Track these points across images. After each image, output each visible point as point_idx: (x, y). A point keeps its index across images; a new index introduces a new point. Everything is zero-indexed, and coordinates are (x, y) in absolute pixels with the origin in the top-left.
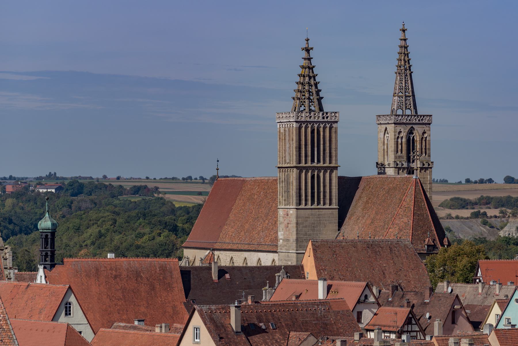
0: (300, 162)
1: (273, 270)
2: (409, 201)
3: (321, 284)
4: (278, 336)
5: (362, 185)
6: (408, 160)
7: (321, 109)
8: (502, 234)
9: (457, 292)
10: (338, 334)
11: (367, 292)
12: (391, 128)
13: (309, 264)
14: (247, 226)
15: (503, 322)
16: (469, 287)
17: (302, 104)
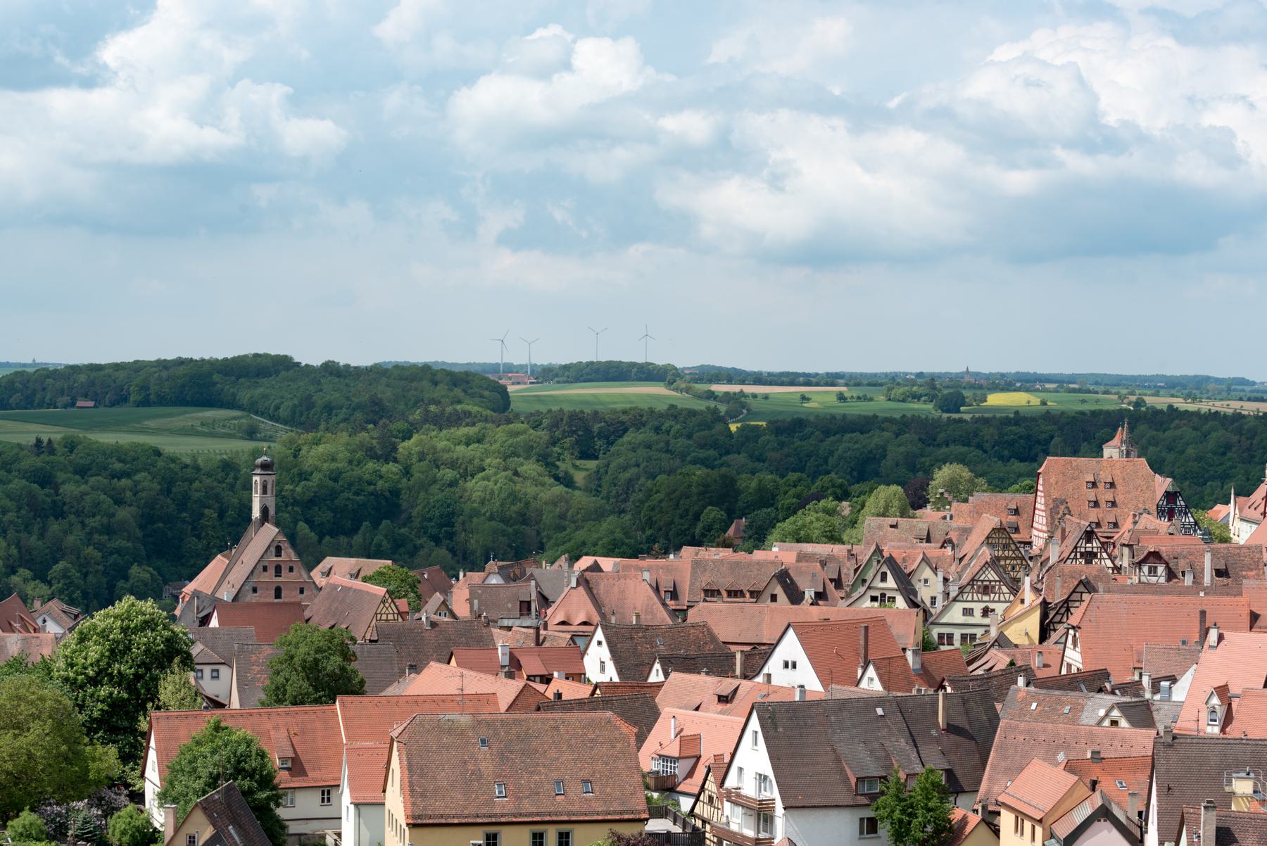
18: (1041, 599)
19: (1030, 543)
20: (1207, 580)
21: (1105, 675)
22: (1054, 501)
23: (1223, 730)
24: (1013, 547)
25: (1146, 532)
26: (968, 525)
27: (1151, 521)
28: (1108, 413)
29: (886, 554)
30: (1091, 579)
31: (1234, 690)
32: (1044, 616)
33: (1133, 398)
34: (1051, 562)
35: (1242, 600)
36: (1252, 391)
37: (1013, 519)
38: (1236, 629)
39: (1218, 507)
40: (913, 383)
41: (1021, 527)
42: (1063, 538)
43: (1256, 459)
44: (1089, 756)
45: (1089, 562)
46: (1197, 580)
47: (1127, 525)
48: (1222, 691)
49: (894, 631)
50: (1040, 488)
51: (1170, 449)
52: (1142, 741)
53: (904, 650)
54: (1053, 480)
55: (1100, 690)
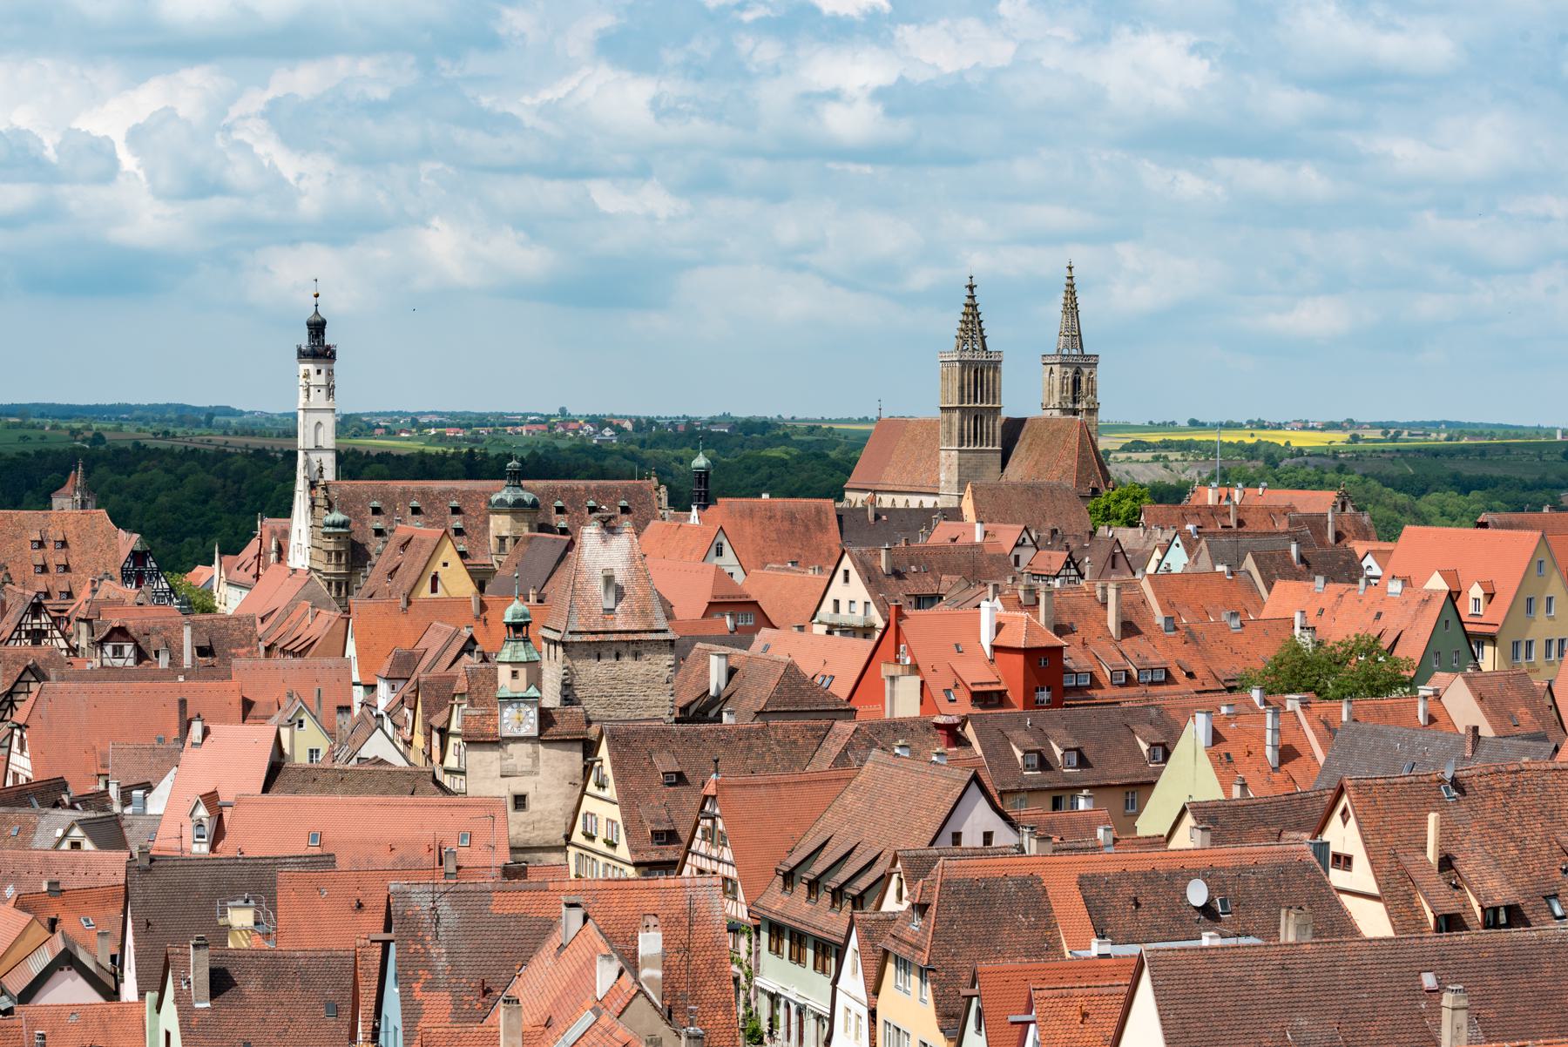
0: (962, 402)
1: (934, 510)
2: (1074, 441)
3: (978, 526)
4: (929, 579)
5: (1027, 426)
6: (1075, 401)
7: (984, 348)
8: (1183, 478)
9: (1118, 536)
10: (992, 578)
11: (1025, 535)
12: (1056, 368)
13: (968, 507)
14: (909, 468)
15: (1163, 565)
16: (1131, 531)
17: (965, 342)
20: (187, 660)
21: (61, 785)
23: (213, 849)
25: (109, 602)
27: (113, 589)
28: (58, 454)
31: (225, 796)
33: (89, 434)
35: (232, 685)
36: (242, 425)
38: (224, 720)
39: (199, 569)
43: (246, 508)
44: (45, 888)
45: (36, 642)
46: (175, 661)
47: (83, 595)
48: (211, 799)
51: (137, 497)
52: (111, 866)
55: (56, 805)
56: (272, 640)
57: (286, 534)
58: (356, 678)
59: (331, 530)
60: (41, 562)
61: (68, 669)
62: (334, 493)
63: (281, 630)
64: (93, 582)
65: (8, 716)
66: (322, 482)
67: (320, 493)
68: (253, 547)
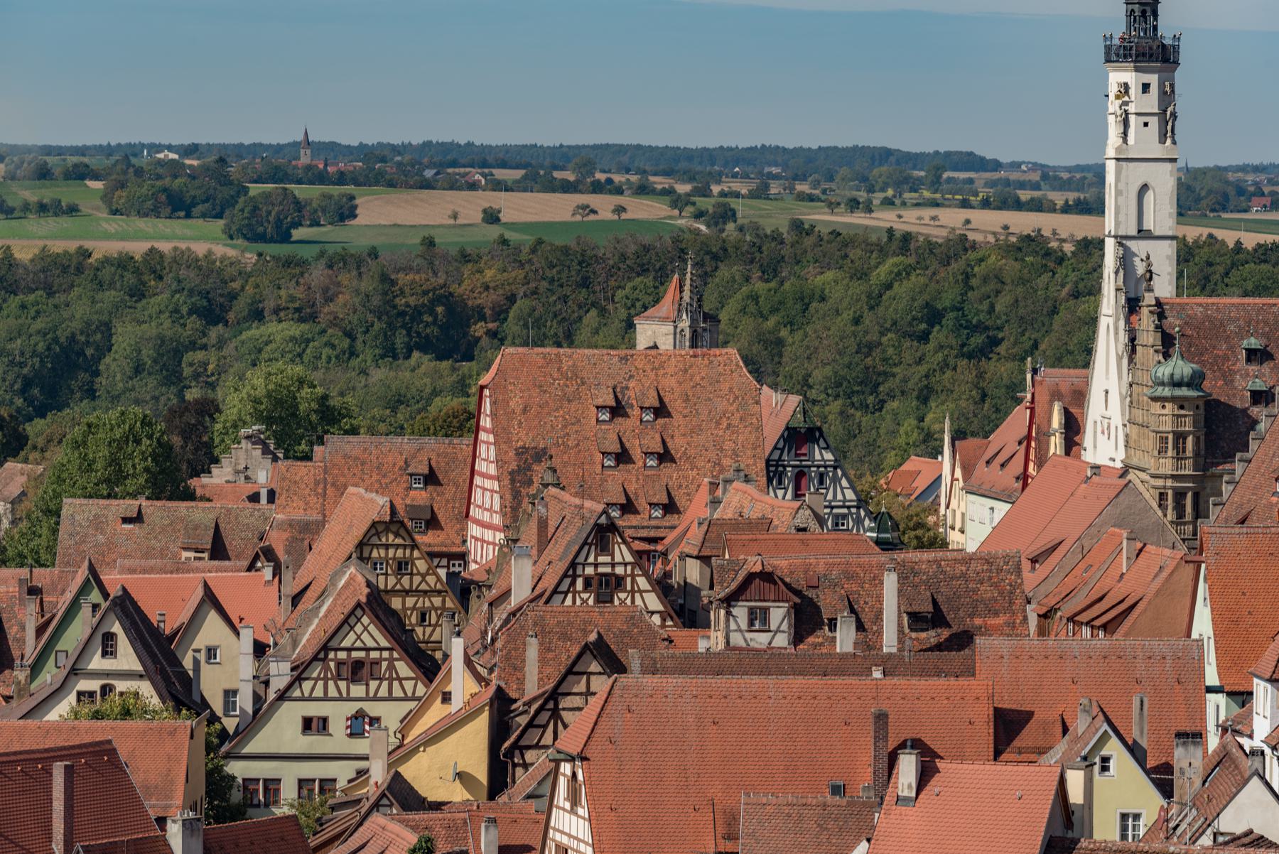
18: (492, 690)
19: (463, 557)
20: (889, 642)
22: (521, 452)
24: (421, 565)
25: (742, 524)
26: (314, 516)
29: (114, 591)
30: (610, 639)
32: (499, 730)
34: (514, 601)
35: (976, 685)
36: (991, 184)
37: (420, 496)
40: (175, 168)
41: (441, 516)
42: (544, 541)
43: (1002, 349)
47: (696, 509)
49: (136, 778)
50: (486, 422)
53: (162, 821)
54: (515, 403)
56: (1052, 602)
57: (1080, 396)
58: (1212, 678)
59: (1167, 392)
60: (616, 448)
61: (662, 650)
62: (1174, 323)
63: (1070, 582)
64: (714, 486)
65: (548, 739)
66: (1149, 299)
67: (1146, 320)
68: (1017, 421)
